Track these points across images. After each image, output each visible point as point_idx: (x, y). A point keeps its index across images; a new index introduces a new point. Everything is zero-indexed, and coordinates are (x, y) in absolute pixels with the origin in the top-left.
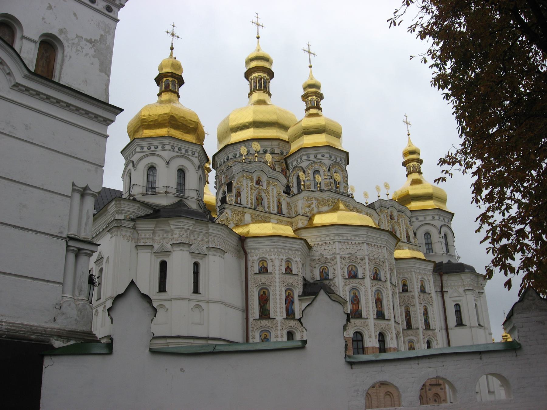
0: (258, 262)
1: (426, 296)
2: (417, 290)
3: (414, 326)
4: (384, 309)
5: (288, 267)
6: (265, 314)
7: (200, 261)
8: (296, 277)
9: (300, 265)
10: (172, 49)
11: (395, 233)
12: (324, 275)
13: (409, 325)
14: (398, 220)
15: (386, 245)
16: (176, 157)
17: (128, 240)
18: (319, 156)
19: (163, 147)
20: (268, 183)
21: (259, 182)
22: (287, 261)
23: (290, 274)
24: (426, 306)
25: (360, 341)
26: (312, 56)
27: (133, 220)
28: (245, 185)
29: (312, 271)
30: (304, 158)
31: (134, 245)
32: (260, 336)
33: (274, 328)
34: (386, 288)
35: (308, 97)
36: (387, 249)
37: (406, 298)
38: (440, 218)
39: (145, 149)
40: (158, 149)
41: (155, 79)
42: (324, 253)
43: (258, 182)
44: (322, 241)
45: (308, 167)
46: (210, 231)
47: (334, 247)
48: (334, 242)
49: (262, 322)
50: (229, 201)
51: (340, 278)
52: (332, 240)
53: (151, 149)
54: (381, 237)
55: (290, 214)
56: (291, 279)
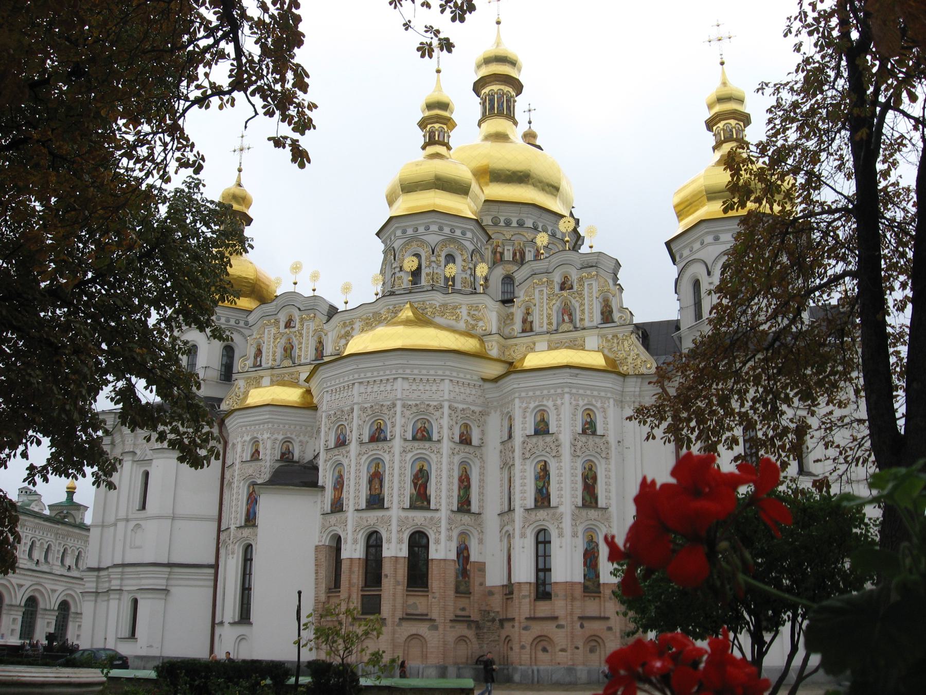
1: (540, 441)
9: (269, 444)
10: (240, 170)
11: (571, 314)
20: (302, 320)
23: (257, 459)
24: (545, 462)
38: (717, 239)
44: (423, 375)
54: (387, 363)
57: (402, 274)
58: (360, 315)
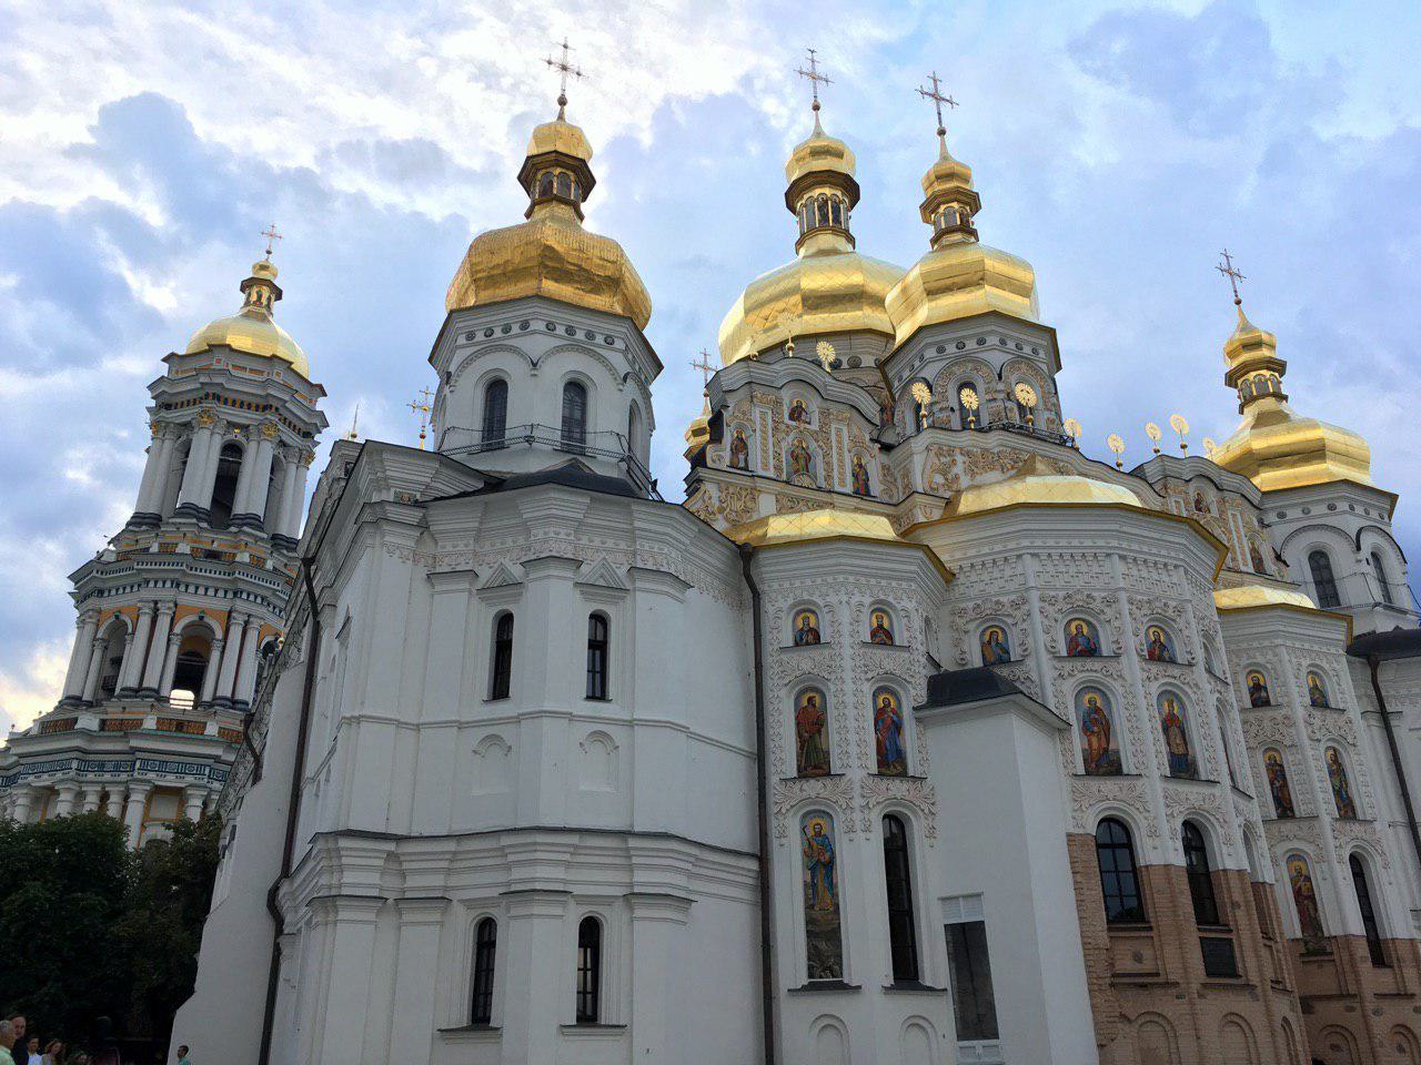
0: (791, 617)
1: (1331, 717)
2: (1300, 699)
3: (1300, 809)
4: (1193, 748)
5: (880, 627)
6: (814, 762)
7: (610, 610)
8: (906, 655)
9: (918, 623)
10: (562, 102)
12: (997, 652)
13: (1285, 808)
14: (1222, 512)
15: (1187, 564)
16: (559, 349)
17: (404, 559)
18: (971, 345)
19: (525, 325)
20: (825, 413)
21: (800, 415)
22: (872, 611)
23: (885, 644)
25: (1122, 846)
26: (945, 107)
27: (417, 504)
28: (758, 421)
29: (957, 644)
30: (931, 353)
31: (422, 572)
32: (803, 829)
33: (842, 802)
34: (1196, 685)
35: (938, 207)
36: (1186, 572)
37: (1266, 723)
39: (480, 336)
40: (512, 333)
41: (519, 178)
42: (993, 589)
43: (797, 413)
45: (939, 375)
46: (637, 524)
47: (1019, 570)
48: (1019, 557)
49: (805, 787)
50: (714, 461)
51: (1045, 657)
52: (1013, 550)
53: (494, 336)
55: (891, 497)
56: (886, 660)
57: (1009, 404)
58: (964, 444)
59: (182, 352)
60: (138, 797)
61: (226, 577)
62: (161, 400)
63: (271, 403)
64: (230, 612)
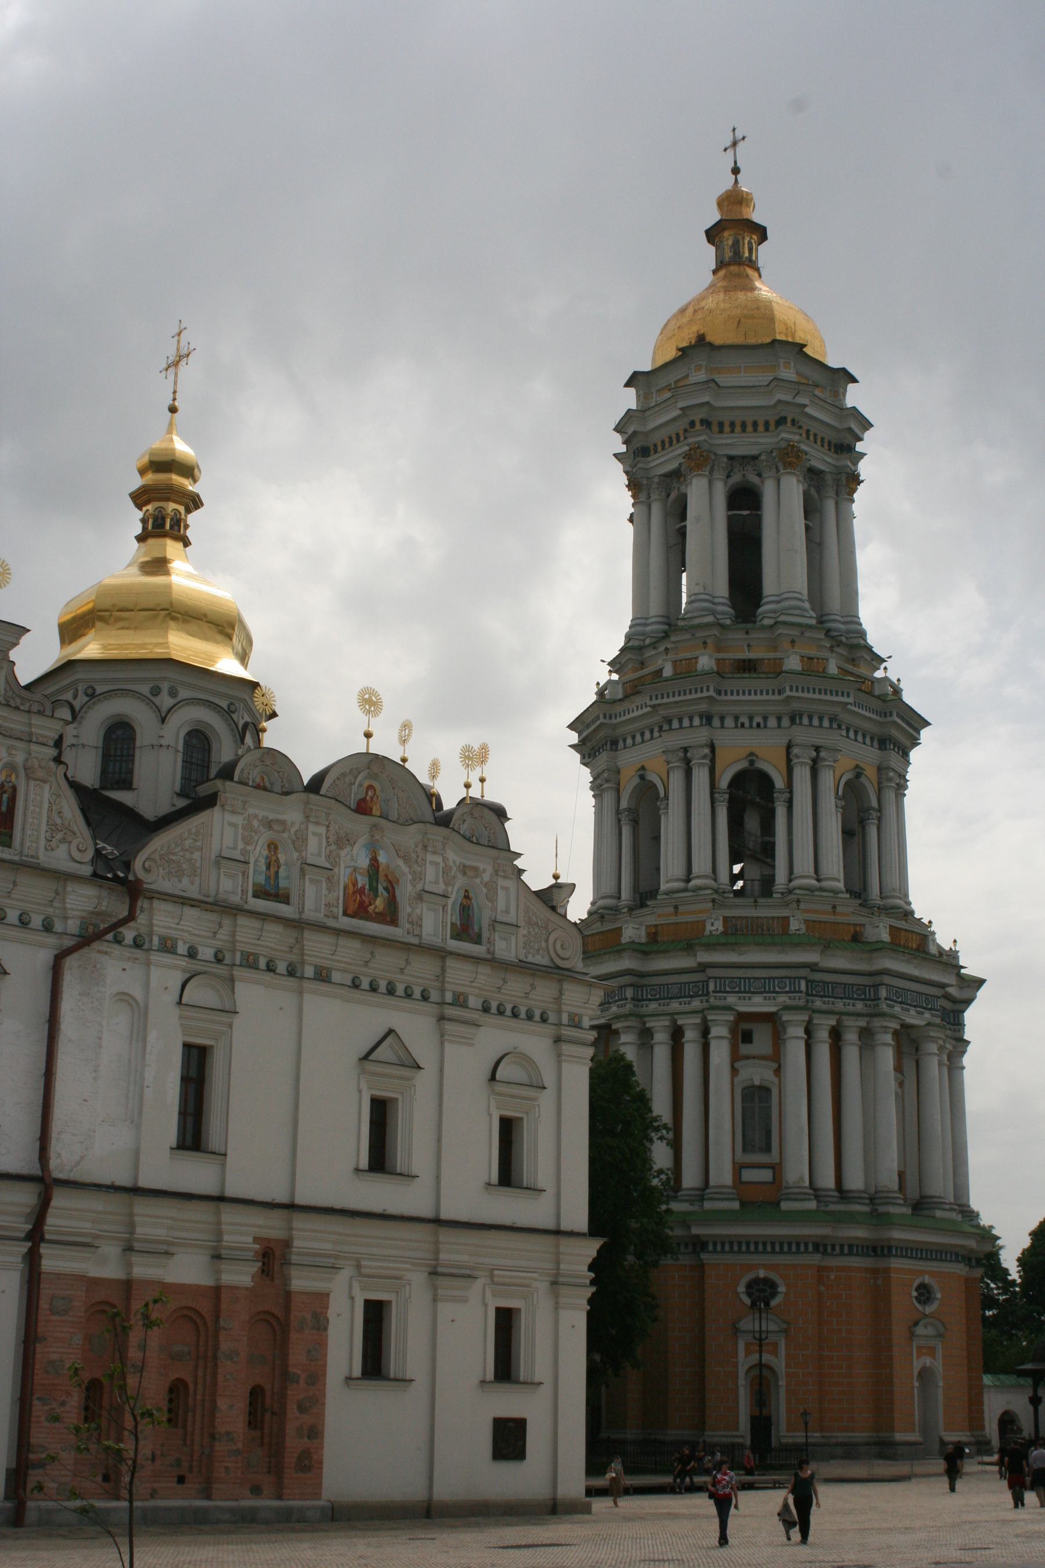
59: (647, 367)
60: (719, 1031)
61: (777, 697)
62: (638, 443)
63: (783, 414)
64: (789, 747)
